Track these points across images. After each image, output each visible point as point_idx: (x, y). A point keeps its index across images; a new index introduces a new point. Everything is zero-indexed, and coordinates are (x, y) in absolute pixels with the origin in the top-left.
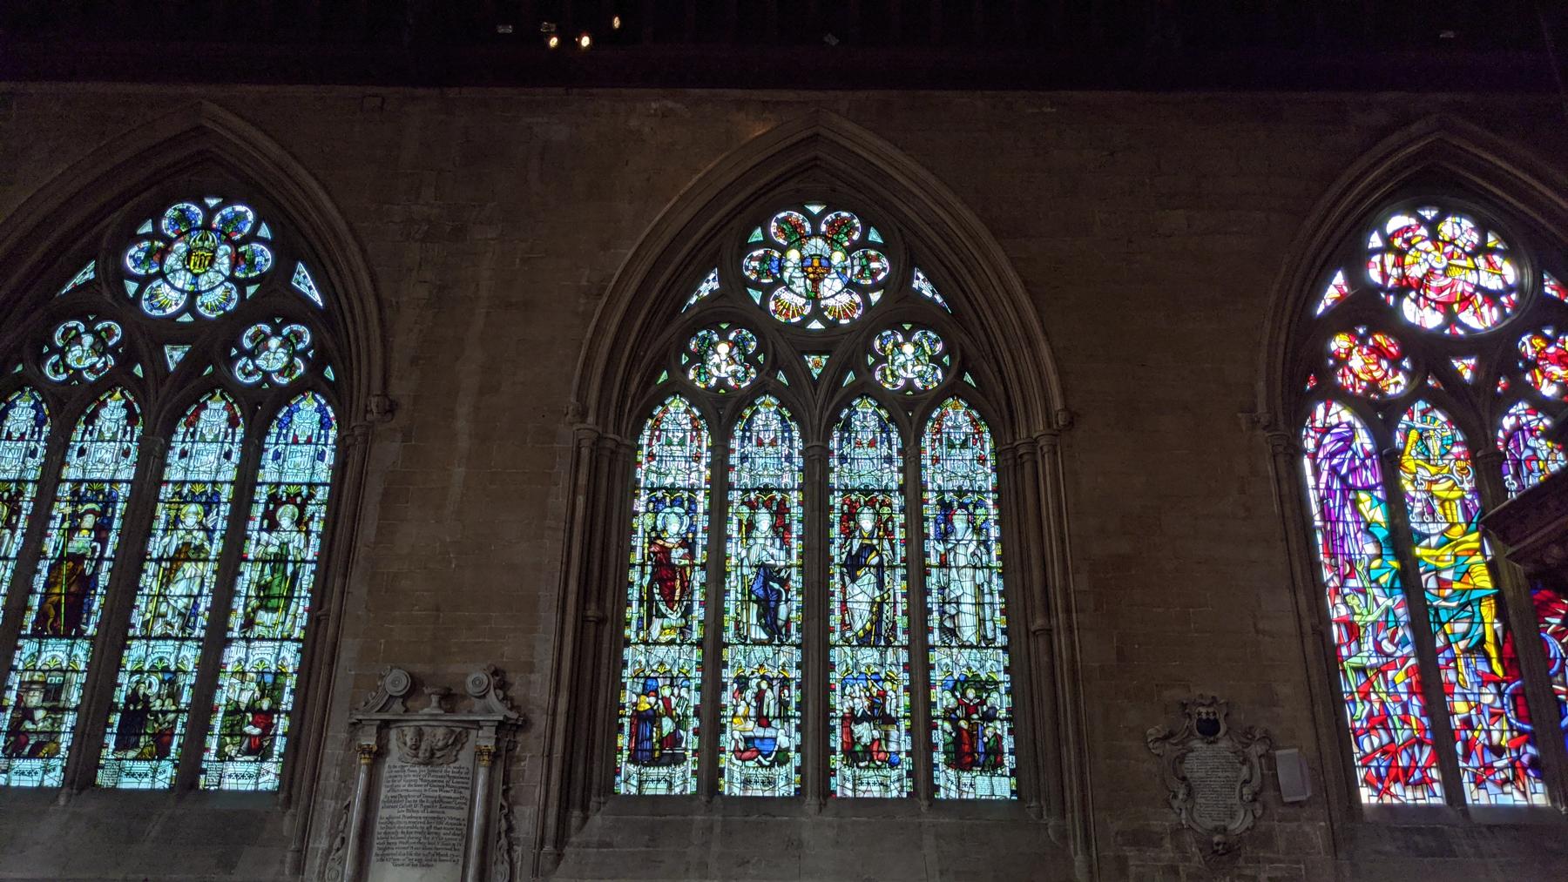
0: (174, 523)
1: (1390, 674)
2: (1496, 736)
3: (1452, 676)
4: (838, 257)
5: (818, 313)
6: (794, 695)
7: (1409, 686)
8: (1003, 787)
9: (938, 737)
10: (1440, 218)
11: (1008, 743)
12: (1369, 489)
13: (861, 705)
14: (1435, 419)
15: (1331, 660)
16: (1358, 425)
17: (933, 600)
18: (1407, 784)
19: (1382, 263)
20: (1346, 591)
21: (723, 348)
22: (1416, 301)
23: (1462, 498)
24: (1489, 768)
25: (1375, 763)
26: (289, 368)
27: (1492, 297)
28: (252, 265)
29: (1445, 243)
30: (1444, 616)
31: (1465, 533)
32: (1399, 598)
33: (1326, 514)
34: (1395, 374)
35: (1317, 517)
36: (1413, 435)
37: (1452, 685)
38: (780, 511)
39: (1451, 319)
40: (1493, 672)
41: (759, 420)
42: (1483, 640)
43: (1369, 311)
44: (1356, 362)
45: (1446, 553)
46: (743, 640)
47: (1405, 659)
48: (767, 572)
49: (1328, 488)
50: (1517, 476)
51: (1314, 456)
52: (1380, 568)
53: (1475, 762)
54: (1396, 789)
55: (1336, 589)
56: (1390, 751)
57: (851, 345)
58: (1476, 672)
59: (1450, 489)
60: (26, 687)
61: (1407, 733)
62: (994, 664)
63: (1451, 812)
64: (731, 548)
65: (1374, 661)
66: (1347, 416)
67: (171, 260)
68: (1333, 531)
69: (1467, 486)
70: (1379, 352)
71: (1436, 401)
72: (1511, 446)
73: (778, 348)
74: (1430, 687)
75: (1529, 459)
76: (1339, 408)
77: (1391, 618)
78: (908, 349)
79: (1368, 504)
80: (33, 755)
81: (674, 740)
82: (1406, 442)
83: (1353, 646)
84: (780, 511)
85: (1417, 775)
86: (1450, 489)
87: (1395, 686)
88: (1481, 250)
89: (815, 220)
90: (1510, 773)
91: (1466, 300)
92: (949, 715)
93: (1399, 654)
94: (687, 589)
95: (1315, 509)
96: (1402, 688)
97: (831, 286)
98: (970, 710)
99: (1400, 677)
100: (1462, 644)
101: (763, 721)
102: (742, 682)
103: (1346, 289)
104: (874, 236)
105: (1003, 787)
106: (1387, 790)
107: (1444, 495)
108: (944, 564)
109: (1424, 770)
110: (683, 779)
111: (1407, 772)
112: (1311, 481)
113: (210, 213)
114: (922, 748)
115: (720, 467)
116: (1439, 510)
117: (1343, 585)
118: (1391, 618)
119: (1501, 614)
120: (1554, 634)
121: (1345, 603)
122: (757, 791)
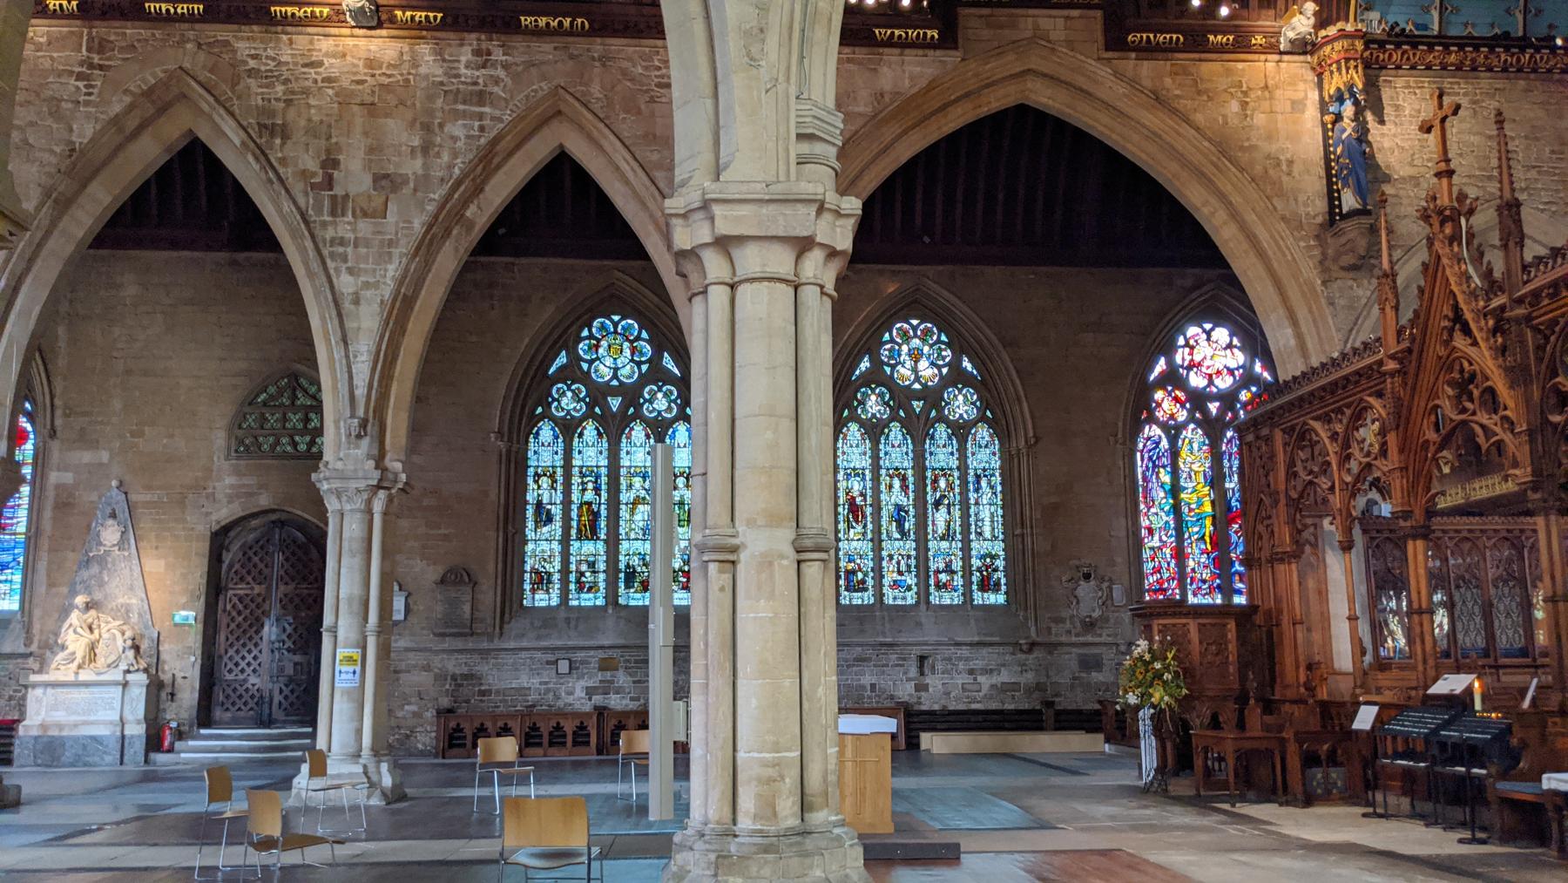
0: (630, 486)
4: (926, 349)
5: (917, 379)
6: (913, 562)
8: (1000, 599)
9: (974, 579)
11: (1003, 581)
12: (1164, 467)
13: (942, 566)
15: (1138, 544)
17: (972, 519)
21: (873, 397)
26: (669, 409)
27: (1231, 372)
28: (642, 354)
33: (1145, 479)
38: (904, 479)
41: (892, 435)
43: (1173, 378)
44: (1166, 405)
45: (1194, 496)
46: (890, 538)
48: (899, 508)
57: (933, 397)
60: (579, 562)
62: (998, 548)
64: (883, 497)
67: (601, 351)
70: (1176, 399)
71: (1199, 424)
73: (899, 397)
74: (1180, 555)
78: (961, 398)
80: (590, 590)
81: (863, 582)
84: (904, 479)
88: (1230, 346)
89: (915, 328)
91: (1219, 373)
92: (979, 569)
94: (864, 516)
97: (923, 364)
98: (988, 567)
99: (1168, 551)
101: (900, 573)
102: (891, 557)
104: (944, 338)
105: (1000, 599)
108: (977, 503)
110: (867, 598)
113: (616, 325)
114: (968, 584)
115: (876, 458)
119: (1214, 524)
122: (899, 602)
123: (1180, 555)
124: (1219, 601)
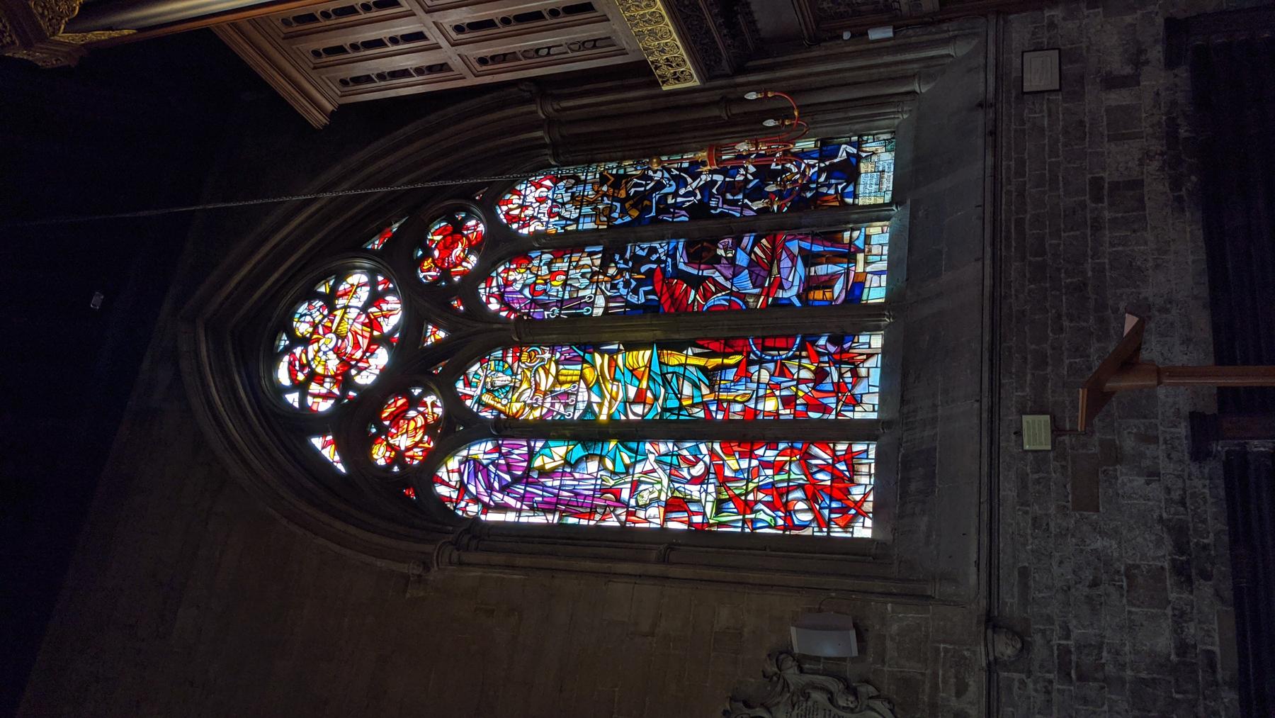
1: (728, 473)
2: (805, 374)
3: (738, 408)
7: (743, 456)
10: (291, 333)
12: (531, 454)
14: (476, 373)
15: (702, 538)
16: (465, 453)
18: (851, 481)
19: (315, 396)
20: (633, 502)
22: (360, 370)
23: (557, 363)
24: (839, 388)
25: (826, 512)
27: (376, 298)
29: (315, 331)
30: (673, 403)
31: (593, 366)
32: (648, 446)
33: (548, 507)
34: (425, 405)
35: (550, 517)
36: (487, 398)
37: (746, 410)
39: (385, 340)
40: (736, 365)
42: (703, 369)
44: (403, 442)
47: (712, 453)
49: (522, 499)
50: (546, 306)
51: (486, 508)
52: (614, 462)
53: (831, 401)
54: (857, 493)
55: (629, 514)
56: (813, 493)
58: (736, 382)
59: (547, 372)
61: (794, 468)
63: (884, 439)
65: (711, 488)
66: (453, 463)
68: (567, 504)
69: (547, 355)
71: (460, 370)
72: (517, 306)
74: (747, 433)
75: (533, 292)
76: (444, 469)
77: (668, 459)
79: (547, 460)
82: (493, 408)
83: (693, 508)
85: (842, 467)
86: (547, 372)
87: (740, 470)
90: (845, 368)
91: (373, 324)
93: (707, 459)
95: (539, 519)
96: (744, 464)
99: (732, 463)
100: (705, 391)
103: (329, 438)
106: (858, 505)
107: (551, 379)
109: (837, 459)
111: (836, 476)
112: (511, 517)
116: (565, 387)
117: (627, 505)
118: (668, 459)
119: (679, 347)
120: (706, 299)
121: (645, 507)
123: (747, 433)
124: (877, 341)
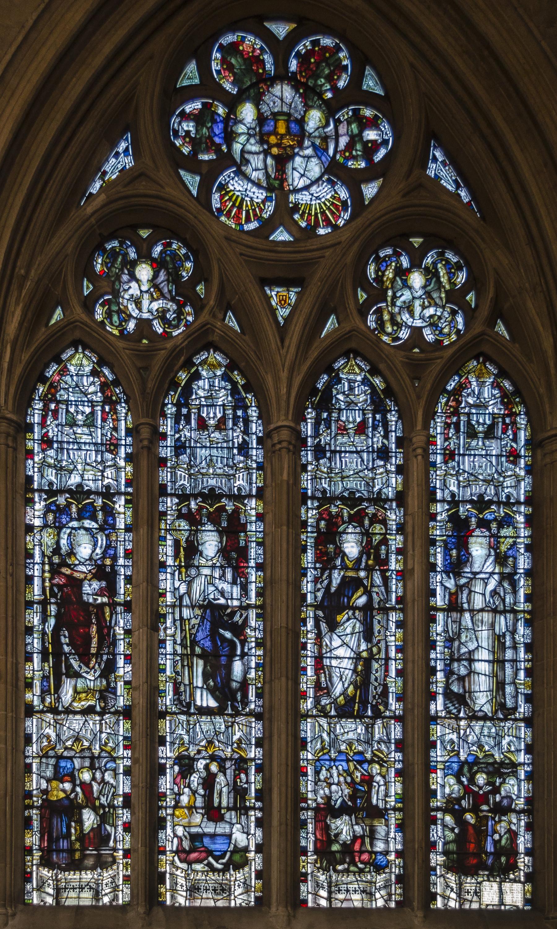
4: (314, 118)
5: (285, 212)
6: (253, 781)
8: (515, 895)
9: (437, 833)
11: (523, 842)
13: (340, 793)
17: (438, 655)
21: (144, 272)
38: (232, 530)
41: (201, 388)
46: (186, 707)
48: (216, 615)
57: (334, 273)
62: (513, 741)
64: (167, 582)
73: (223, 273)
78: (417, 280)
81: (100, 838)
84: (232, 530)
89: (281, 49)
92: (451, 806)
94: (107, 639)
97: (305, 169)
98: (479, 799)
101: (214, 814)
102: (186, 765)
104: (371, 83)
105: (515, 895)
108: (454, 606)
110: (110, 885)
114: (416, 851)
115: (146, 456)
122: (207, 900)
